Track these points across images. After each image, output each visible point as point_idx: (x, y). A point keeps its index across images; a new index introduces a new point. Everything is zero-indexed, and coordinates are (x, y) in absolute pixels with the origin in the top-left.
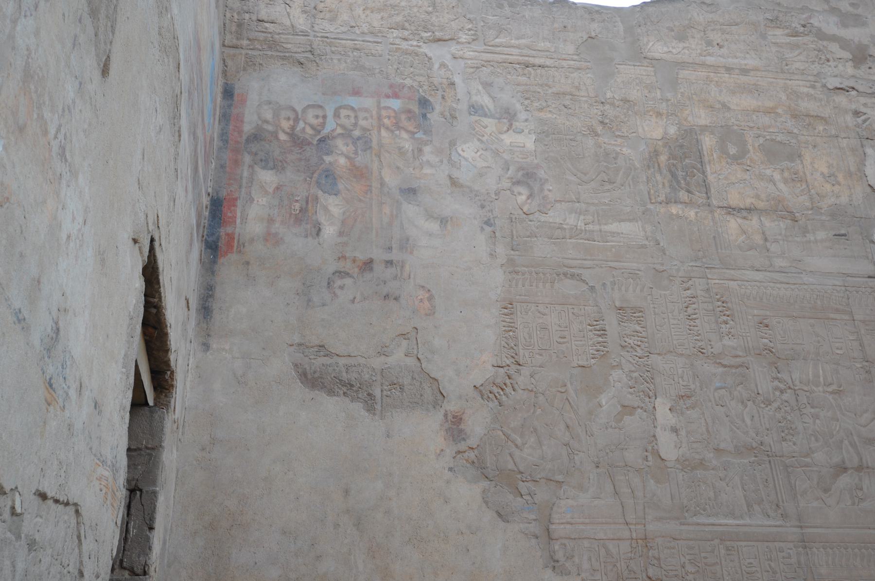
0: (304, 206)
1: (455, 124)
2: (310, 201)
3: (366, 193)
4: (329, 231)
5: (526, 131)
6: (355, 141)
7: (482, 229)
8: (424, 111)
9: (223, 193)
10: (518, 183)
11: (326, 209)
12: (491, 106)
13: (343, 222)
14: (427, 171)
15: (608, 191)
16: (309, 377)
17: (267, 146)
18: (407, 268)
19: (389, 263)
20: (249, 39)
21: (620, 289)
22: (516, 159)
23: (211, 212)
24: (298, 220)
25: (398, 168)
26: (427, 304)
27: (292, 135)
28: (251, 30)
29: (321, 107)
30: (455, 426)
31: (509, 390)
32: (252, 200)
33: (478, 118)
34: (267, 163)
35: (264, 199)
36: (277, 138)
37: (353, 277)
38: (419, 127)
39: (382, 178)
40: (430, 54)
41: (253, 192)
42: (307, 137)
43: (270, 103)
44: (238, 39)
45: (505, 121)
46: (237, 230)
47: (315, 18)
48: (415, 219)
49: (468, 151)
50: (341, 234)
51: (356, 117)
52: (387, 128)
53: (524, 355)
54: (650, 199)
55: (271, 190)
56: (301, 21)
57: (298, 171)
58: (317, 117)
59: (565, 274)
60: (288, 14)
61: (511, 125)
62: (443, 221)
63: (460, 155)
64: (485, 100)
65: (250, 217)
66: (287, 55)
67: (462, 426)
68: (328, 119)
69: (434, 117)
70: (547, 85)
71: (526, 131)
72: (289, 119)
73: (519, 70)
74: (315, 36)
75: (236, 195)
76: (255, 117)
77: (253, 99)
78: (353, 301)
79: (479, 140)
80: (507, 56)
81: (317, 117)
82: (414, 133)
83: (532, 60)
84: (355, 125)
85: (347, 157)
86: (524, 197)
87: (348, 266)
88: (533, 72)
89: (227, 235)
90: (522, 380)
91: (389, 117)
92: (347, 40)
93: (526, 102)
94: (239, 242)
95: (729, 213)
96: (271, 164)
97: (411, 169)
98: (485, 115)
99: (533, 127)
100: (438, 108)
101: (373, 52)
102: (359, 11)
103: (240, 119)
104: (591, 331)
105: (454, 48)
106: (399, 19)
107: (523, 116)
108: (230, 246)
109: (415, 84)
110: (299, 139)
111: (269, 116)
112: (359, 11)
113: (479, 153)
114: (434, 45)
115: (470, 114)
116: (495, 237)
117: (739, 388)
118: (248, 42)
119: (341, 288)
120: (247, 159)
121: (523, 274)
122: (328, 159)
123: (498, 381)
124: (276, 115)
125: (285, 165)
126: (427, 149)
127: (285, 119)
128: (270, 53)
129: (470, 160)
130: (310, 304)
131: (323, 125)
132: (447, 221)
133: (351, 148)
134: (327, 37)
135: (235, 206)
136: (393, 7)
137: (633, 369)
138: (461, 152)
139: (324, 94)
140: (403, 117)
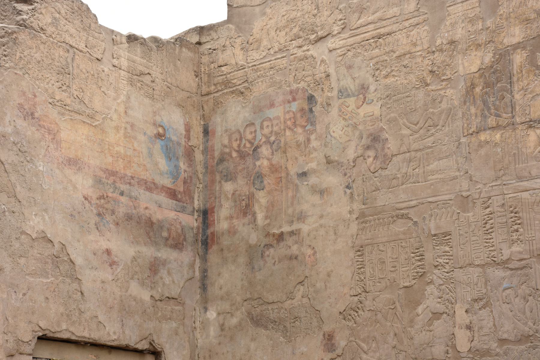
0: (247, 202)
1: (330, 110)
2: (251, 197)
4: (260, 216)
5: (375, 100)
7: (345, 192)
9: (208, 205)
10: (368, 148)
12: (352, 87)
13: (267, 209)
15: (433, 135)
16: (255, 319)
17: (227, 164)
20: (215, 85)
21: (435, 219)
23: (203, 220)
24: (245, 214)
28: (215, 77)
30: (329, 341)
31: (360, 312)
34: (229, 177)
36: (231, 157)
40: (315, 55)
41: (222, 200)
42: (247, 150)
44: (209, 87)
45: (361, 96)
46: (216, 228)
50: (266, 217)
52: (290, 128)
54: (463, 133)
55: (230, 196)
56: (241, 57)
57: (244, 177)
58: (251, 133)
59: (397, 216)
61: (365, 98)
62: (322, 192)
63: (331, 136)
65: (221, 218)
66: (234, 88)
69: (317, 109)
70: (393, 51)
71: (375, 100)
72: (236, 140)
73: (373, 44)
77: (219, 130)
78: (274, 264)
79: (344, 119)
80: (365, 35)
83: (382, 31)
85: (268, 159)
86: (371, 159)
89: (212, 233)
90: (368, 303)
92: (266, 62)
93: (377, 73)
95: (530, 127)
97: (303, 157)
98: (349, 96)
99: (379, 96)
101: (281, 66)
102: (273, 33)
104: (413, 257)
105: (330, 43)
106: (295, 30)
107: (372, 88)
108: (213, 240)
110: (243, 152)
111: (226, 142)
112: (273, 33)
113: (344, 131)
114: (319, 44)
115: (339, 98)
117: (523, 287)
120: (218, 178)
121: (370, 221)
122: (258, 163)
123: (353, 306)
124: (230, 140)
126: (313, 137)
128: (225, 91)
129: (338, 138)
130: (254, 270)
131: (255, 138)
133: (270, 150)
134: (255, 65)
135: (214, 212)
136: (292, 20)
137: (442, 282)
138: (332, 134)
139: (254, 113)
140: (299, 115)
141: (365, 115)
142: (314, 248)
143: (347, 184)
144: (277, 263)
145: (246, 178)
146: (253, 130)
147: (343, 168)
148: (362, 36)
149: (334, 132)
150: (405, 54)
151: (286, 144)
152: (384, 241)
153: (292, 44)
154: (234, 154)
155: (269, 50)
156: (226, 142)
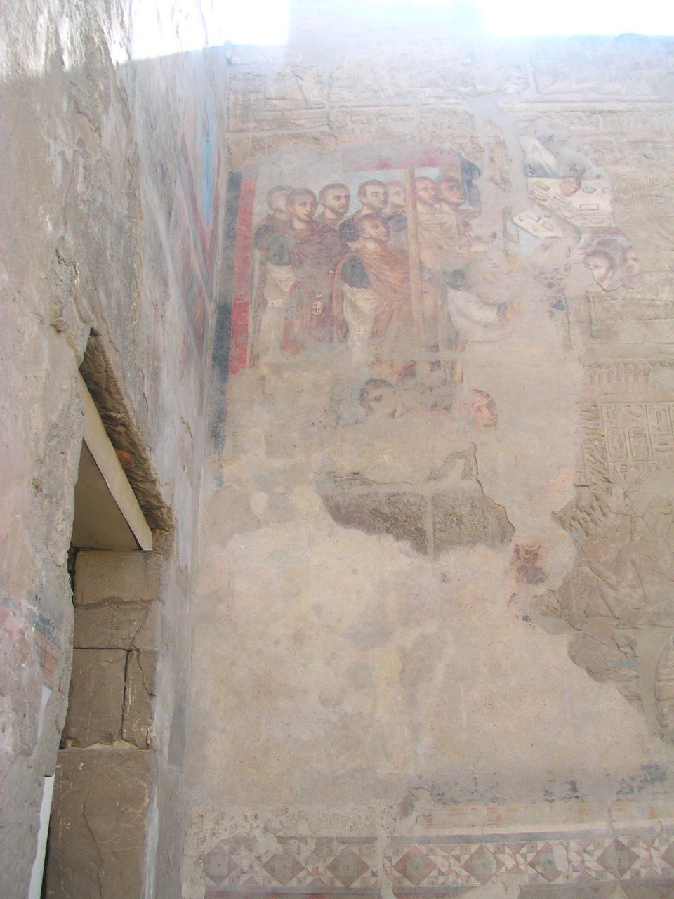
3: (403, 282)
5: (599, 190)
6: (386, 221)
8: (468, 177)
10: (594, 253)
11: (354, 306)
13: (376, 320)
14: (478, 248)
16: (343, 511)
18: (458, 368)
19: (436, 364)
20: (255, 121)
22: (590, 224)
23: (218, 322)
25: (441, 248)
26: (486, 413)
27: (310, 222)
28: (259, 110)
29: (341, 186)
30: (529, 565)
31: (597, 514)
32: (265, 303)
33: (536, 179)
34: (281, 257)
35: (280, 301)
36: (291, 226)
37: (390, 385)
38: (463, 196)
39: (421, 262)
41: (266, 294)
43: (281, 188)
45: (572, 179)
47: (331, 87)
48: (467, 309)
49: (528, 220)
50: (374, 334)
51: (386, 193)
52: (424, 203)
53: (615, 469)
55: (287, 290)
57: (319, 263)
58: (338, 198)
60: (300, 87)
64: (547, 160)
66: (300, 132)
67: (538, 564)
68: (352, 199)
69: (481, 183)
70: (622, 133)
71: (599, 190)
74: (332, 107)
75: (246, 299)
76: (266, 207)
77: (262, 185)
78: (393, 415)
79: (540, 205)
80: (568, 105)
81: (338, 198)
82: (458, 205)
84: (385, 202)
85: (376, 240)
86: (602, 271)
87: (384, 372)
88: (601, 119)
90: (615, 501)
91: (426, 189)
94: (251, 355)
96: (286, 259)
97: (457, 248)
98: (546, 175)
100: (486, 174)
103: (249, 213)
108: (242, 360)
109: (455, 148)
113: (541, 222)
116: (569, 322)
118: (255, 124)
119: (378, 399)
120: (258, 255)
122: (353, 245)
123: (583, 504)
124: (290, 202)
125: (303, 258)
127: (300, 205)
128: (280, 132)
129: (531, 231)
130: (341, 422)
131: (346, 207)
132: (506, 308)
134: (346, 107)
135: (245, 311)
139: (345, 171)
141: (583, 207)
142: (488, 395)
143: (555, 301)
144: (398, 413)
145: (326, 265)
146: (343, 194)
147: (543, 276)
148: (563, 105)
149: (521, 220)
150: (644, 142)
151: (417, 224)
152: (640, 399)
153: (424, 92)
154: (299, 225)
155: (375, 91)
156: (281, 203)
